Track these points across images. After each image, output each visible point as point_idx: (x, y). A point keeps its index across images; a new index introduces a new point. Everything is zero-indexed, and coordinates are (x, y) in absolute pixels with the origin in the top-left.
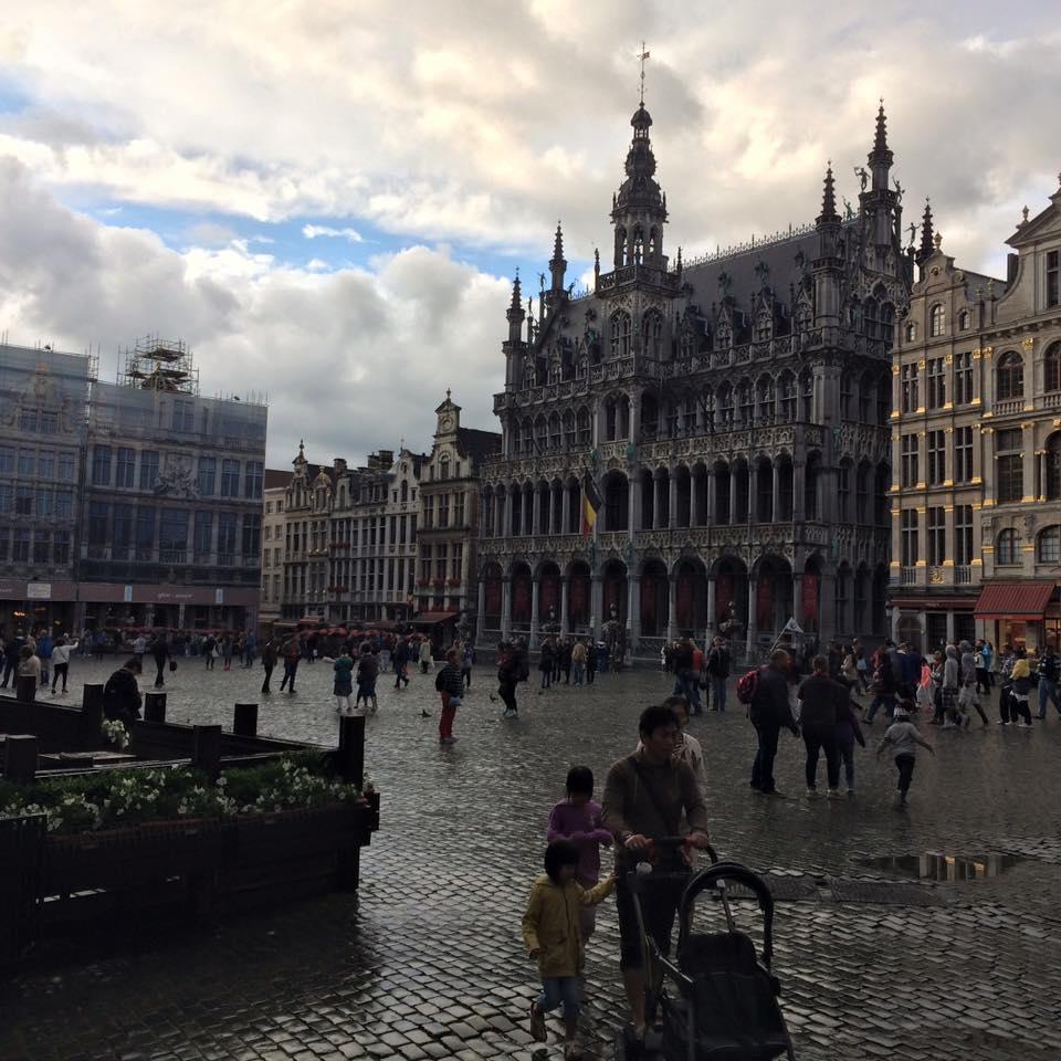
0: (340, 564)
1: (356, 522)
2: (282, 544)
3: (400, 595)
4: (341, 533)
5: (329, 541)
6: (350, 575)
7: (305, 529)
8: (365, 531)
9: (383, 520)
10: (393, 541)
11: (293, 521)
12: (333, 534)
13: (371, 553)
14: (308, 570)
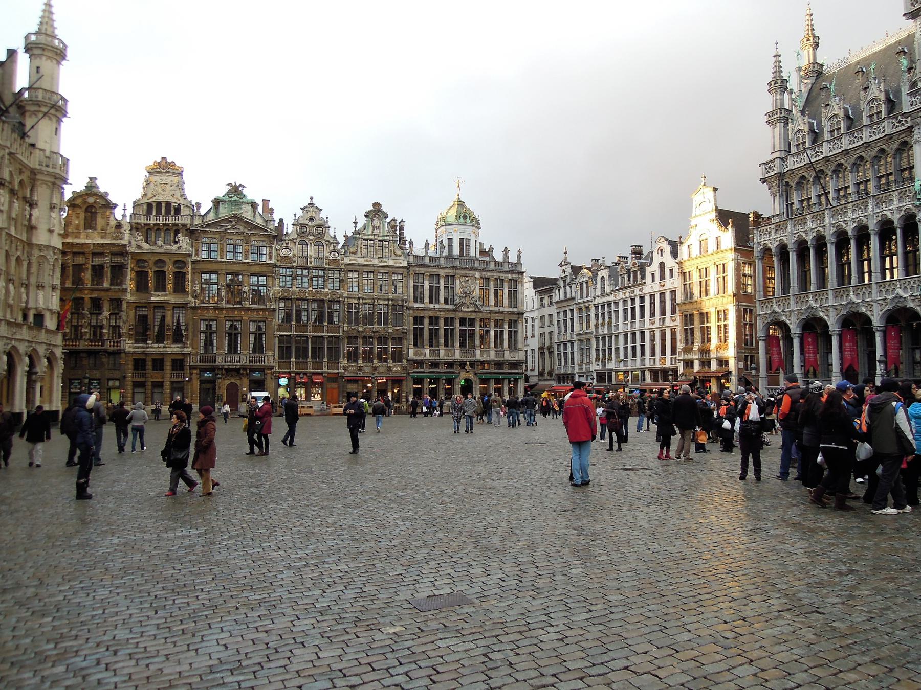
0: (604, 338)
1: (616, 303)
2: (555, 329)
3: (663, 360)
4: (603, 314)
5: (593, 322)
6: (614, 346)
7: (572, 314)
8: (625, 310)
9: (642, 299)
10: (653, 314)
11: (561, 310)
12: (597, 315)
13: (632, 327)
14: (575, 344)
